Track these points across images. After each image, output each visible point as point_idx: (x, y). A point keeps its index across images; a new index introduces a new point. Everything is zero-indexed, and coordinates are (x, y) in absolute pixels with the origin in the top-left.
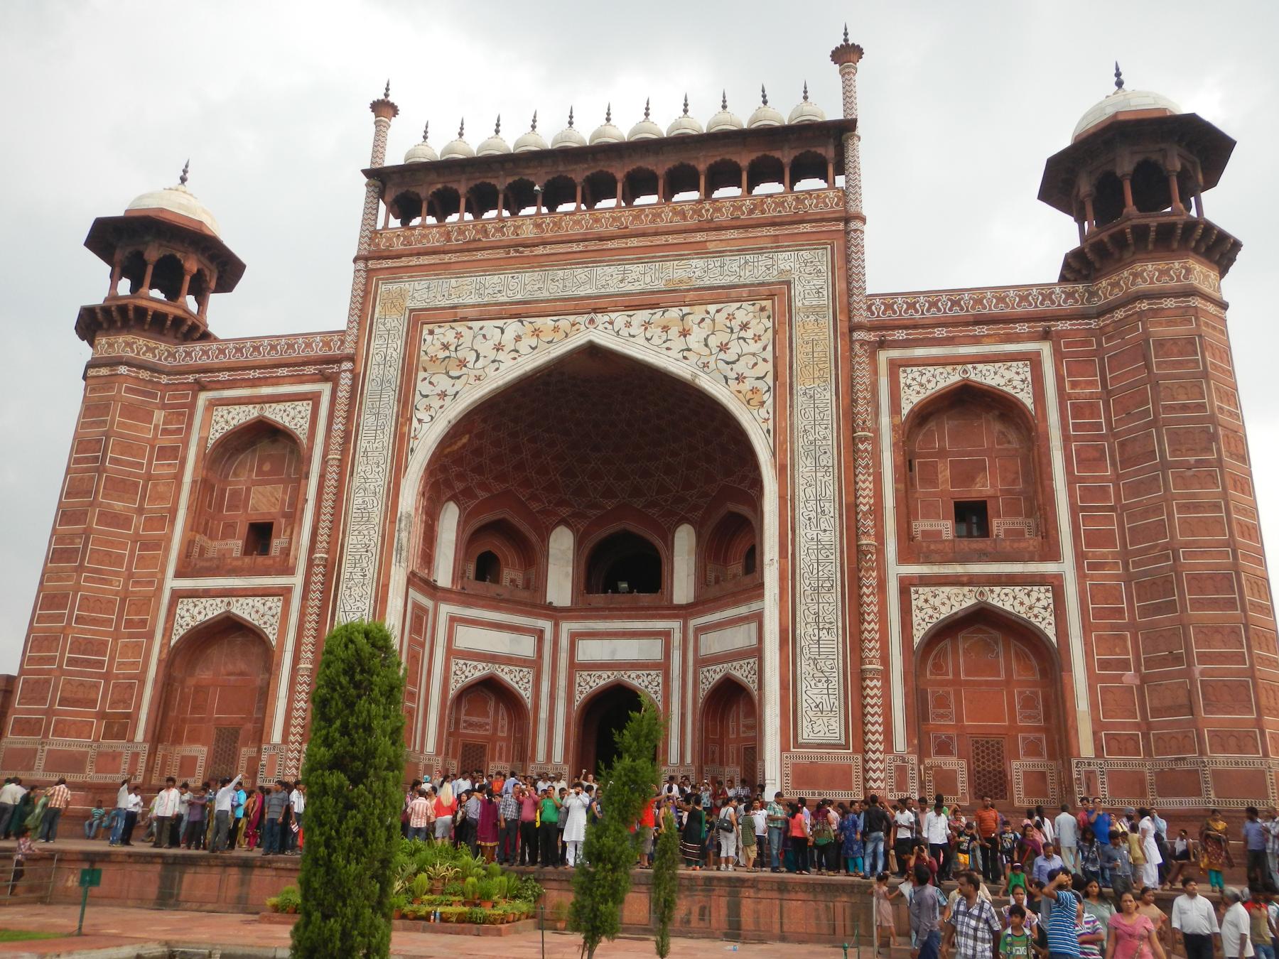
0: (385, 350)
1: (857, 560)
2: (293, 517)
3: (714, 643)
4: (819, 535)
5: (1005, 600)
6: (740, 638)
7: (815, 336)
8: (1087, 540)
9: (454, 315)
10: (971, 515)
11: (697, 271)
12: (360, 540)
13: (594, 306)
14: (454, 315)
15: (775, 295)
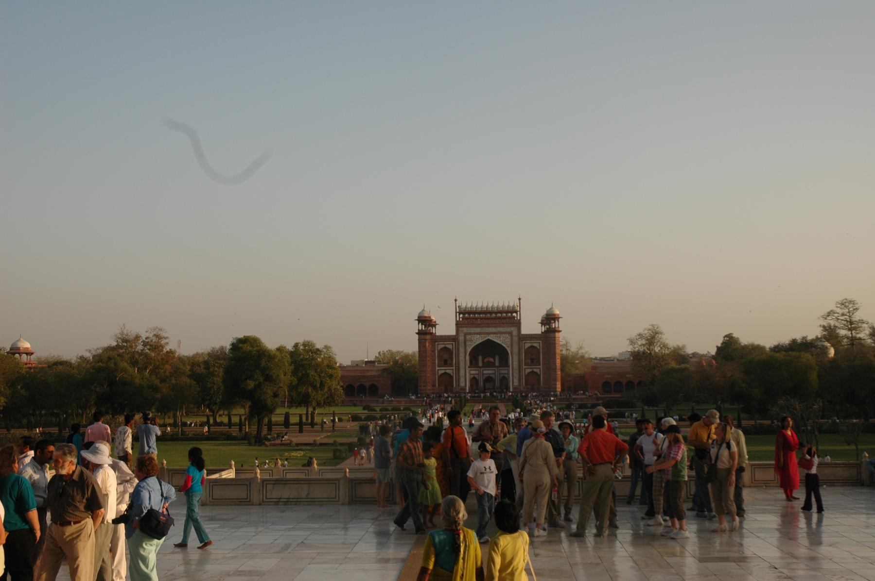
0: (461, 338)
1: (519, 367)
2: (452, 360)
3: (502, 372)
4: (516, 363)
5: (535, 370)
6: (506, 372)
7: (516, 339)
8: (544, 364)
9: (470, 334)
10: (532, 360)
11: (501, 329)
12: (462, 363)
13: (489, 334)
14: (470, 334)
15: (511, 333)
